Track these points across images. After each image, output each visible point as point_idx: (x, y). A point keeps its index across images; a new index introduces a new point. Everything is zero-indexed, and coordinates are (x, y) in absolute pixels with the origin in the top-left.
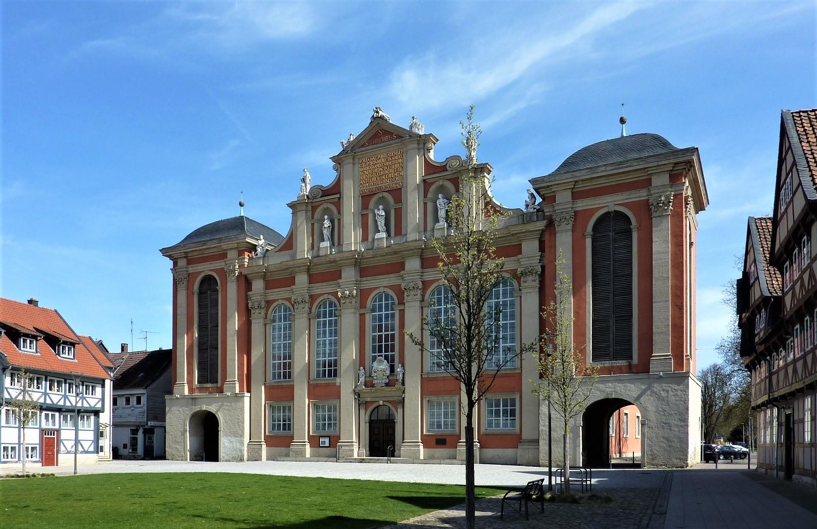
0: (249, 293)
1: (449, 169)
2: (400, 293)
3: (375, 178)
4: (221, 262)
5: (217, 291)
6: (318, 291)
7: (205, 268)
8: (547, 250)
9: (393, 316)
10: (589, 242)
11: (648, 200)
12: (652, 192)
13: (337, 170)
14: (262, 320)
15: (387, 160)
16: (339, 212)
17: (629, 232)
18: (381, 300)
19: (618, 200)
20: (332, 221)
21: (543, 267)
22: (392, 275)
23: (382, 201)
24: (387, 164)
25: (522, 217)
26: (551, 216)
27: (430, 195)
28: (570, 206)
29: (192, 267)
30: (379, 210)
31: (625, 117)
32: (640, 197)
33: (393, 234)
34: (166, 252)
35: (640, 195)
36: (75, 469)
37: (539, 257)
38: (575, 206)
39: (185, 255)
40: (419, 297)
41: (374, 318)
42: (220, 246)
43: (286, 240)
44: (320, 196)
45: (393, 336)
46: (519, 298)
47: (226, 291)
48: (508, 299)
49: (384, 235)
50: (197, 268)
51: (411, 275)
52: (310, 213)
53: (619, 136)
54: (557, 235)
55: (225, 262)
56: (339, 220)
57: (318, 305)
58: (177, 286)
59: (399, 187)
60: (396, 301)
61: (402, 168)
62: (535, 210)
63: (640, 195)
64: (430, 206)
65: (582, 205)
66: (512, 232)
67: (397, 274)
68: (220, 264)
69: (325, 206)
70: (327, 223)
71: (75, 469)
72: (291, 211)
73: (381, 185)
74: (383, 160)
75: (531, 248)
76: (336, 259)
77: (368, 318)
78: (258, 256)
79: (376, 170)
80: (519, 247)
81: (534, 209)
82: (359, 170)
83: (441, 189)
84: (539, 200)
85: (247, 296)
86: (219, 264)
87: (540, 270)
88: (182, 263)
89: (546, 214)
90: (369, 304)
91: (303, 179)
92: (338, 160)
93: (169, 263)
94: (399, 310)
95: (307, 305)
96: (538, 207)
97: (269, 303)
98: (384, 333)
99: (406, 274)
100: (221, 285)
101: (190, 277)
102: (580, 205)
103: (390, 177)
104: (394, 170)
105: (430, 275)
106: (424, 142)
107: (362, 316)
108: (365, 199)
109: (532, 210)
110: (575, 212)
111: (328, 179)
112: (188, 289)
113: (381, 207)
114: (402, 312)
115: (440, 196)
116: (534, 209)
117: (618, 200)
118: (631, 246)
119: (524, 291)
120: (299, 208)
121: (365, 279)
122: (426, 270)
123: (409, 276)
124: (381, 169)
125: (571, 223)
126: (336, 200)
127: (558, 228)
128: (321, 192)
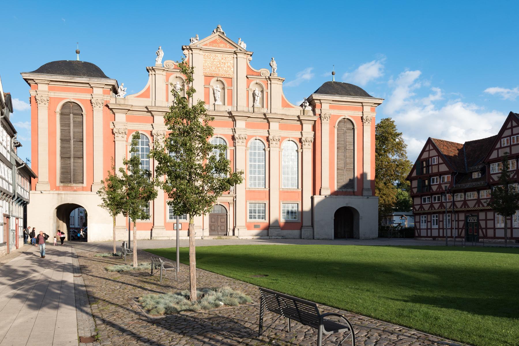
24: (223, 61)
29: (54, 93)
36: (151, 236)
59: (230, 77)
68: (85, 96)
71: (151, 236)
74: (220, 58)
79: (215, 63)
100: (86, 111)
103: (225, 69)
112: (49, 109)
123: (239, 131)
124: (218, 63)
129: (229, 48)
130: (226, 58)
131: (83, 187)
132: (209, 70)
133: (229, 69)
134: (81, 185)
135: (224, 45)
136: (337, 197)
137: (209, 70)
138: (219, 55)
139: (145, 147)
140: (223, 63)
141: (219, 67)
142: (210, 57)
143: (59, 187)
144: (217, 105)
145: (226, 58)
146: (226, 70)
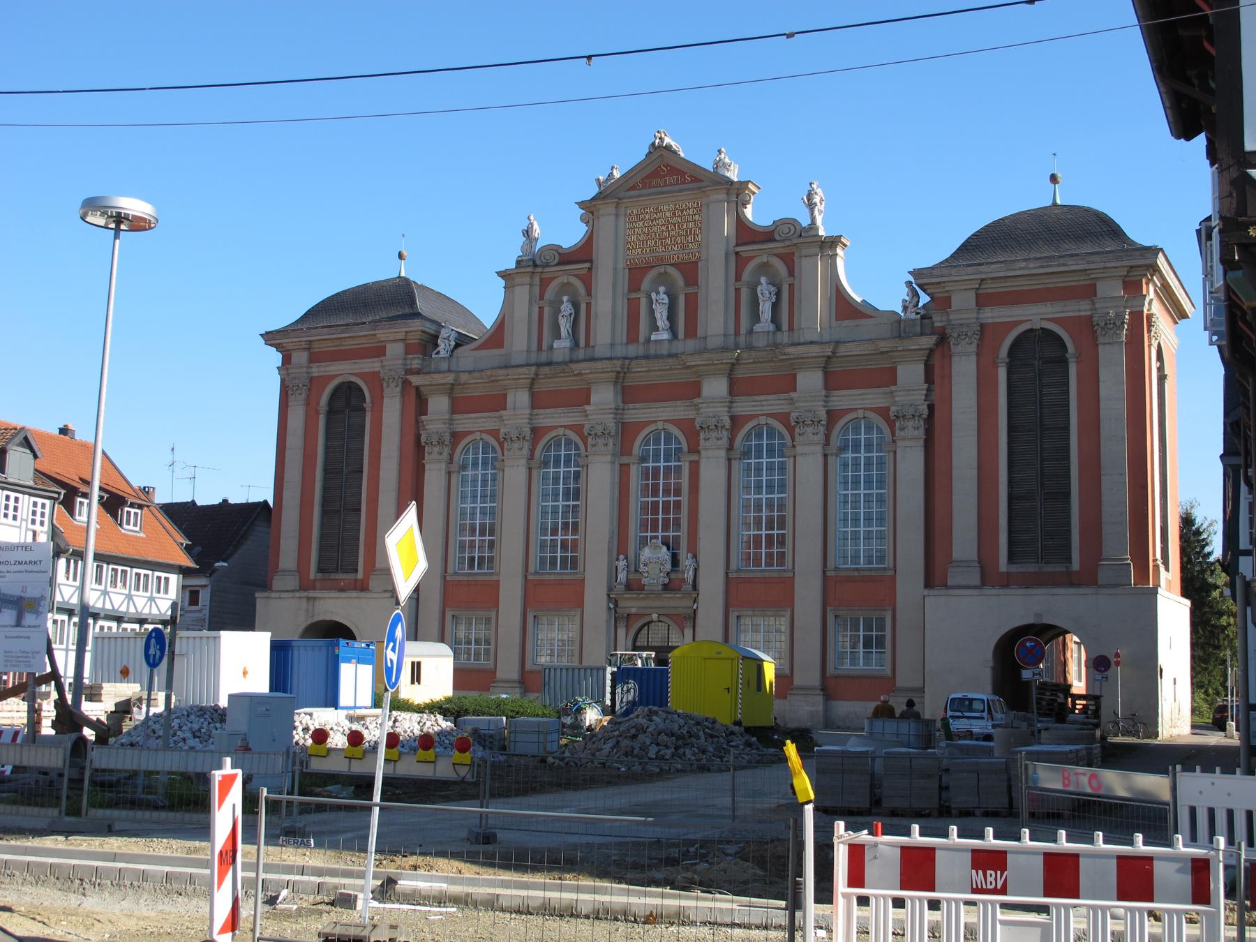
0: (424, 418)
1: (777, 237)
2: (692, 431)
3: (653, 242)
4: (373, 362)
5: (364, 410)
6: (548, 422)
7: (344, 370)
8: (937, 380)
9: (678, 469)
10: (1002, 373)
11: (1091, 317)
12: (1097, 306)
13: (587, 223)
14: (443, 465)
15: (674, 214)
16: (589, 293)
17: (1064, 362)
18: (657, 442)
19: (1047, 313)
20: (576, 305)
21: (931, 408)
22: (679, 403)
23: (663, 278)
24: (674, 220)
25: (897, 327)
26: (944, 328)
27: (746, 275)
28: (975, 315)
30: (658, 293)
31: (1059, 175)
32: (1080, 311)
33: (681, 334)
34: (271, 338)
35: (1080, 308)
37: (925, 392)
38: (981, 316)
39: (307, 346)
40: (725, 442)
41: (645, 474)
42: (375, 335)
43: (489, 334)
44: (556, 261)
45: (678, 504)
46: (892, 455)
47: (381, 411)
48: (875, 454)
49: (665, 336)
50: (328, 369)
51: (711, 405)
52: (537, 290)
53: (1049, 203)
54: (954, 359)
55: (382, 362)
56: (589, 305)
57: (547, 444)
58: (287, 398)
60: (685, 446)
61: (700, 229)
62: (919, 316)
63: (1080, 308)
64: (745, 293)
65: (992, 315)
66: (881, 350)
67: (688, 402)
69: (565, 279)
70: (566, 308)
72: (502, 282)
73: (663, 254)
75: (911, 374)
76: (583, 372)
77: (635, 472)
78: (441, 356)
79: (654, 229)
80: (893, 371)
81: (917, 313)
82: (625, 226)
83: (764, 268)
84: (924, 299)
85: (417, 422)
86: (370, 365)
87: (926, 412)
88: (300, 358)
89: (936, 325)
90: (637, 449)
91: (527, 231)
92: (590, 208)
93: (275, 358)
94: (690, 462)
95: (526, 444)
96: (922, 312)
97: (456, 437)
98: (661, 499)
99: (703, 403)
100: (372, 402)
101: (314, 384)
102: (990, 315)
104: (687, 232)
105: (748, 406)
106: (737, 192)
107: (624, 470)
108: (636, 274)
109: (913, 316)
110: (982, 326)
111: (570, 233)
112: (308, 404)
113: (662, 289)
114: (695, 468)
115: (763, 280)
116: (917, 313)
117: (1047, 313)
118: (1067, 384)
119: (899, 443)
120: (518, 280)
121: (631, 406)
122: (737, 399)
123: (708, 407)
125: (976, 342)
126: (585, 272)
127: (954, 349)
128: (557, 256)
129: (692, 182)
130: (682, 211)
131: (356, 580)
132: (640, 250)
133: (690, 238)
134: (351, 576)
135: (677, 179)
136: (1001, 591)
137: (640, 250)
138: (666, 207)
139: (490, 472)
140: (674, 225)
141: (665, 238)
142: (642, 216)
143: (314, 581)
144: (656, 341)
145: (682, 211)
146: (683, 241)
